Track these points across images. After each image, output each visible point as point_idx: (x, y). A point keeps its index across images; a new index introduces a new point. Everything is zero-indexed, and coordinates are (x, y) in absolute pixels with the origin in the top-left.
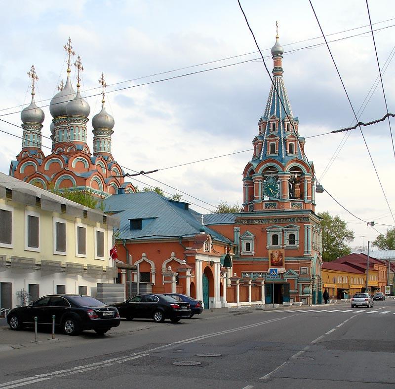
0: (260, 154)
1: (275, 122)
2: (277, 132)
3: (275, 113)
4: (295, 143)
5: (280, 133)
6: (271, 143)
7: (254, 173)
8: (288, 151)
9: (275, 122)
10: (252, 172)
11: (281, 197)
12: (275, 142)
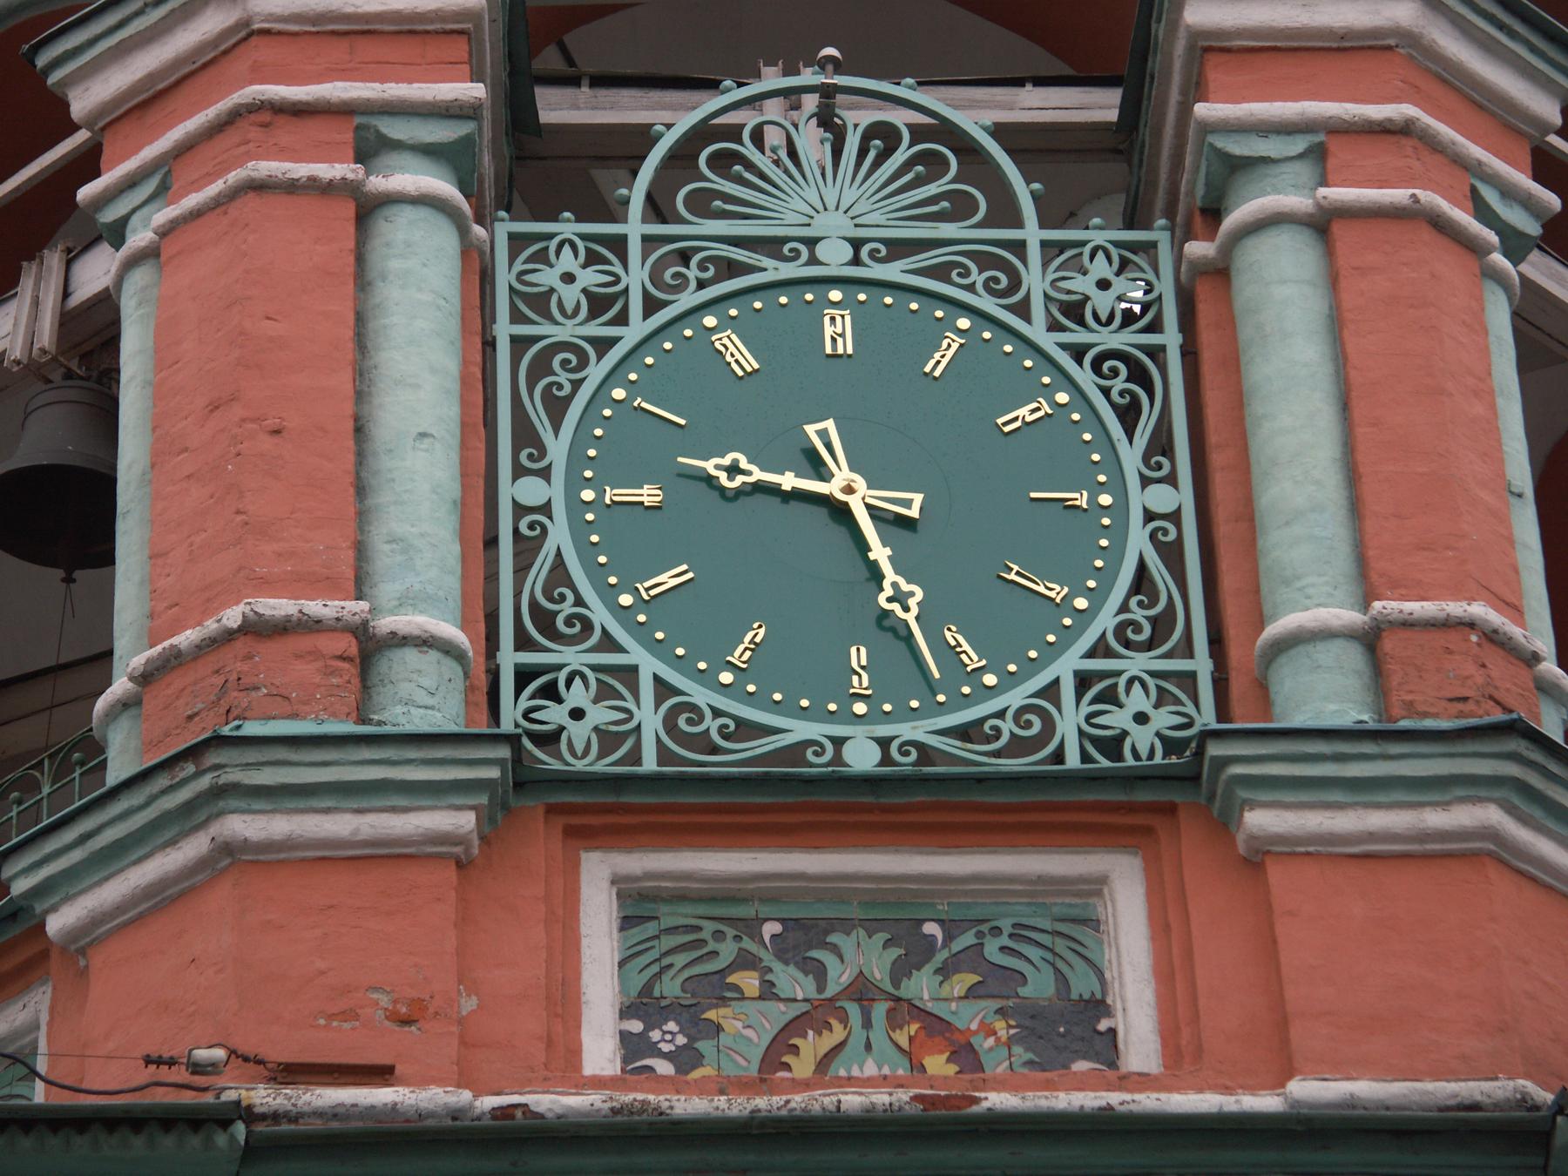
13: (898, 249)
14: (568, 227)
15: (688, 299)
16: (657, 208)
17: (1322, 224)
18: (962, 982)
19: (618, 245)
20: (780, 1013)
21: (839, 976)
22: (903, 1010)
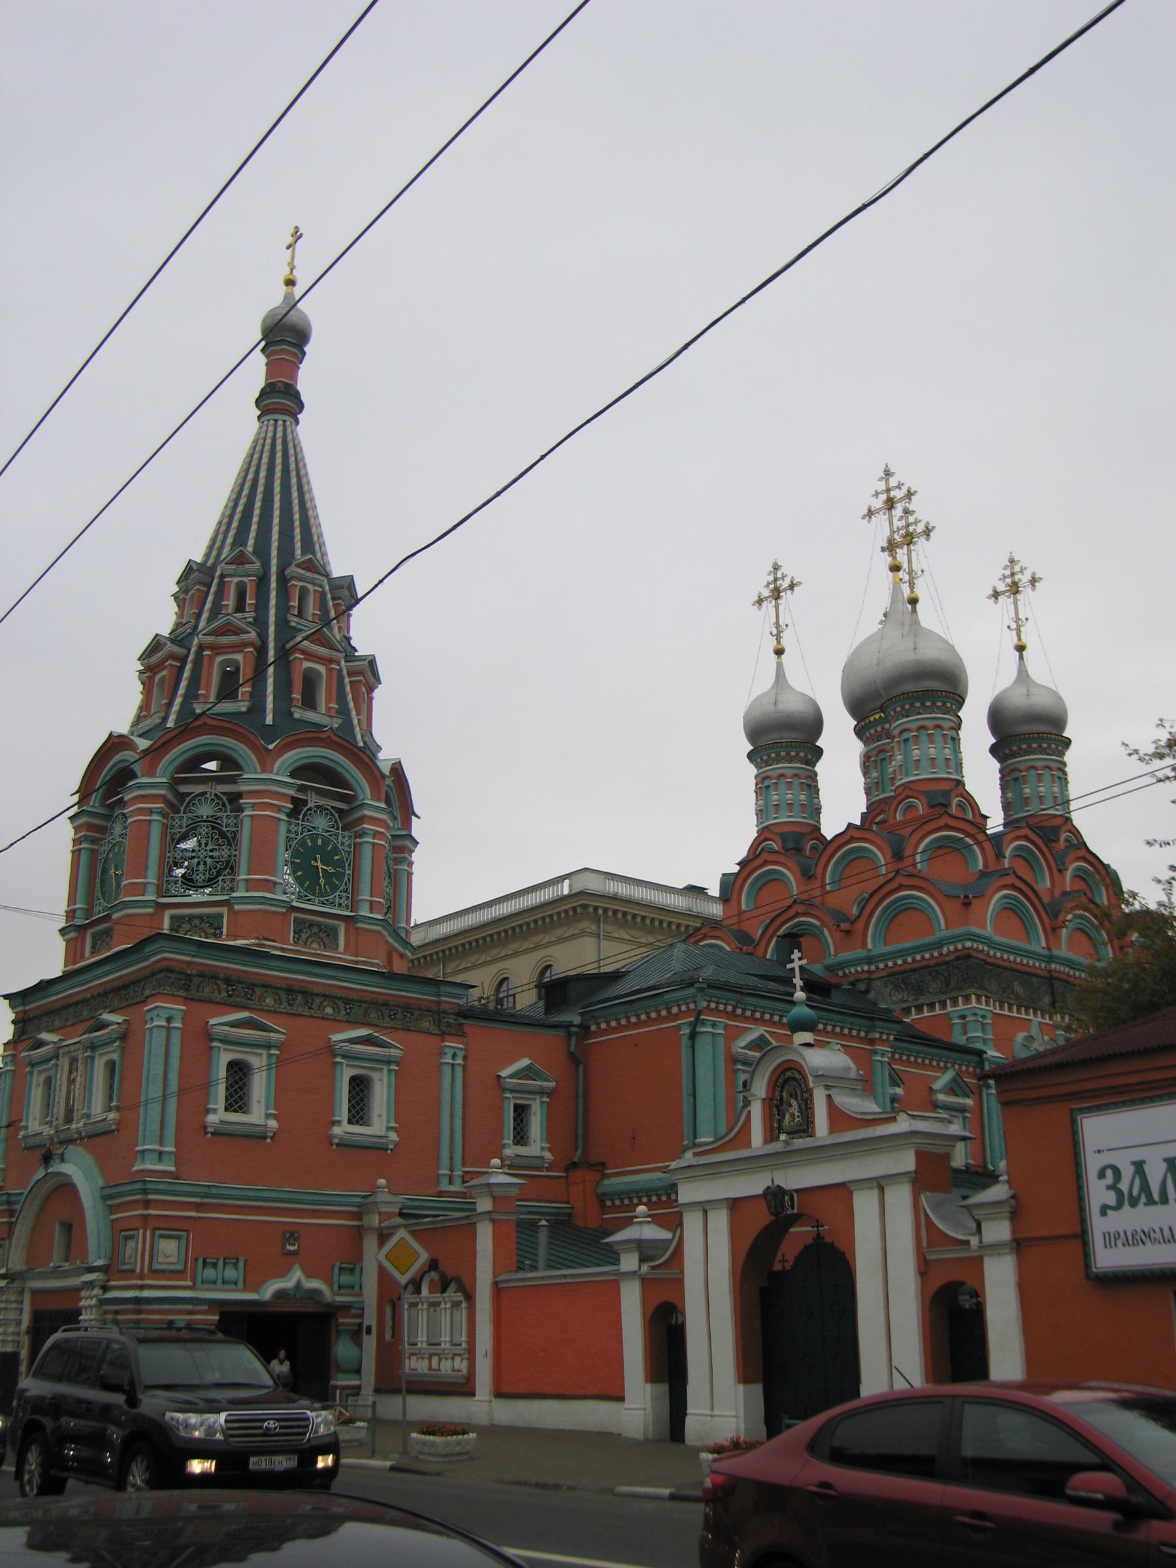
0: (170, 705)
1: (245, 579)
2: (250, 615)
3: (250, 549)
4: (330, 671)
5: (260, 623)
6: (219, 659)
7: (134, 776)
8: (297, 696)
9: (245, 579)
10: (125, 775)
11: (242, 886)
12: (239, 657)
13: (327, 831)
14: (293, 821)
15: (305, 834)
16: (303, 821)
17: (374, 844)
18: (325, 934)
19: (298, 824)
20: (307, 935)
21: (313, 932)
22: (319, 937)
